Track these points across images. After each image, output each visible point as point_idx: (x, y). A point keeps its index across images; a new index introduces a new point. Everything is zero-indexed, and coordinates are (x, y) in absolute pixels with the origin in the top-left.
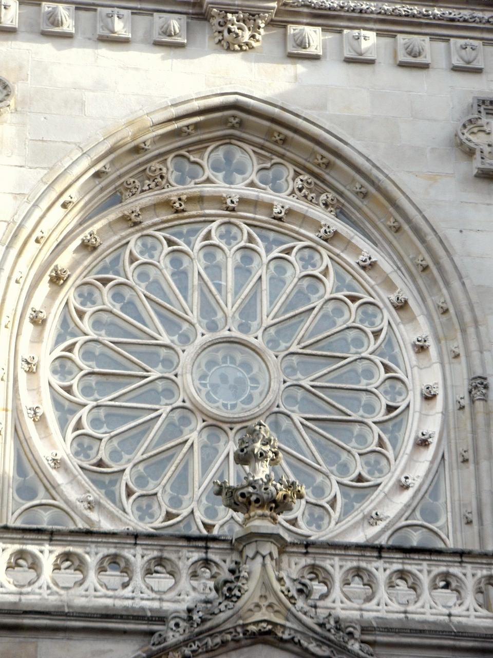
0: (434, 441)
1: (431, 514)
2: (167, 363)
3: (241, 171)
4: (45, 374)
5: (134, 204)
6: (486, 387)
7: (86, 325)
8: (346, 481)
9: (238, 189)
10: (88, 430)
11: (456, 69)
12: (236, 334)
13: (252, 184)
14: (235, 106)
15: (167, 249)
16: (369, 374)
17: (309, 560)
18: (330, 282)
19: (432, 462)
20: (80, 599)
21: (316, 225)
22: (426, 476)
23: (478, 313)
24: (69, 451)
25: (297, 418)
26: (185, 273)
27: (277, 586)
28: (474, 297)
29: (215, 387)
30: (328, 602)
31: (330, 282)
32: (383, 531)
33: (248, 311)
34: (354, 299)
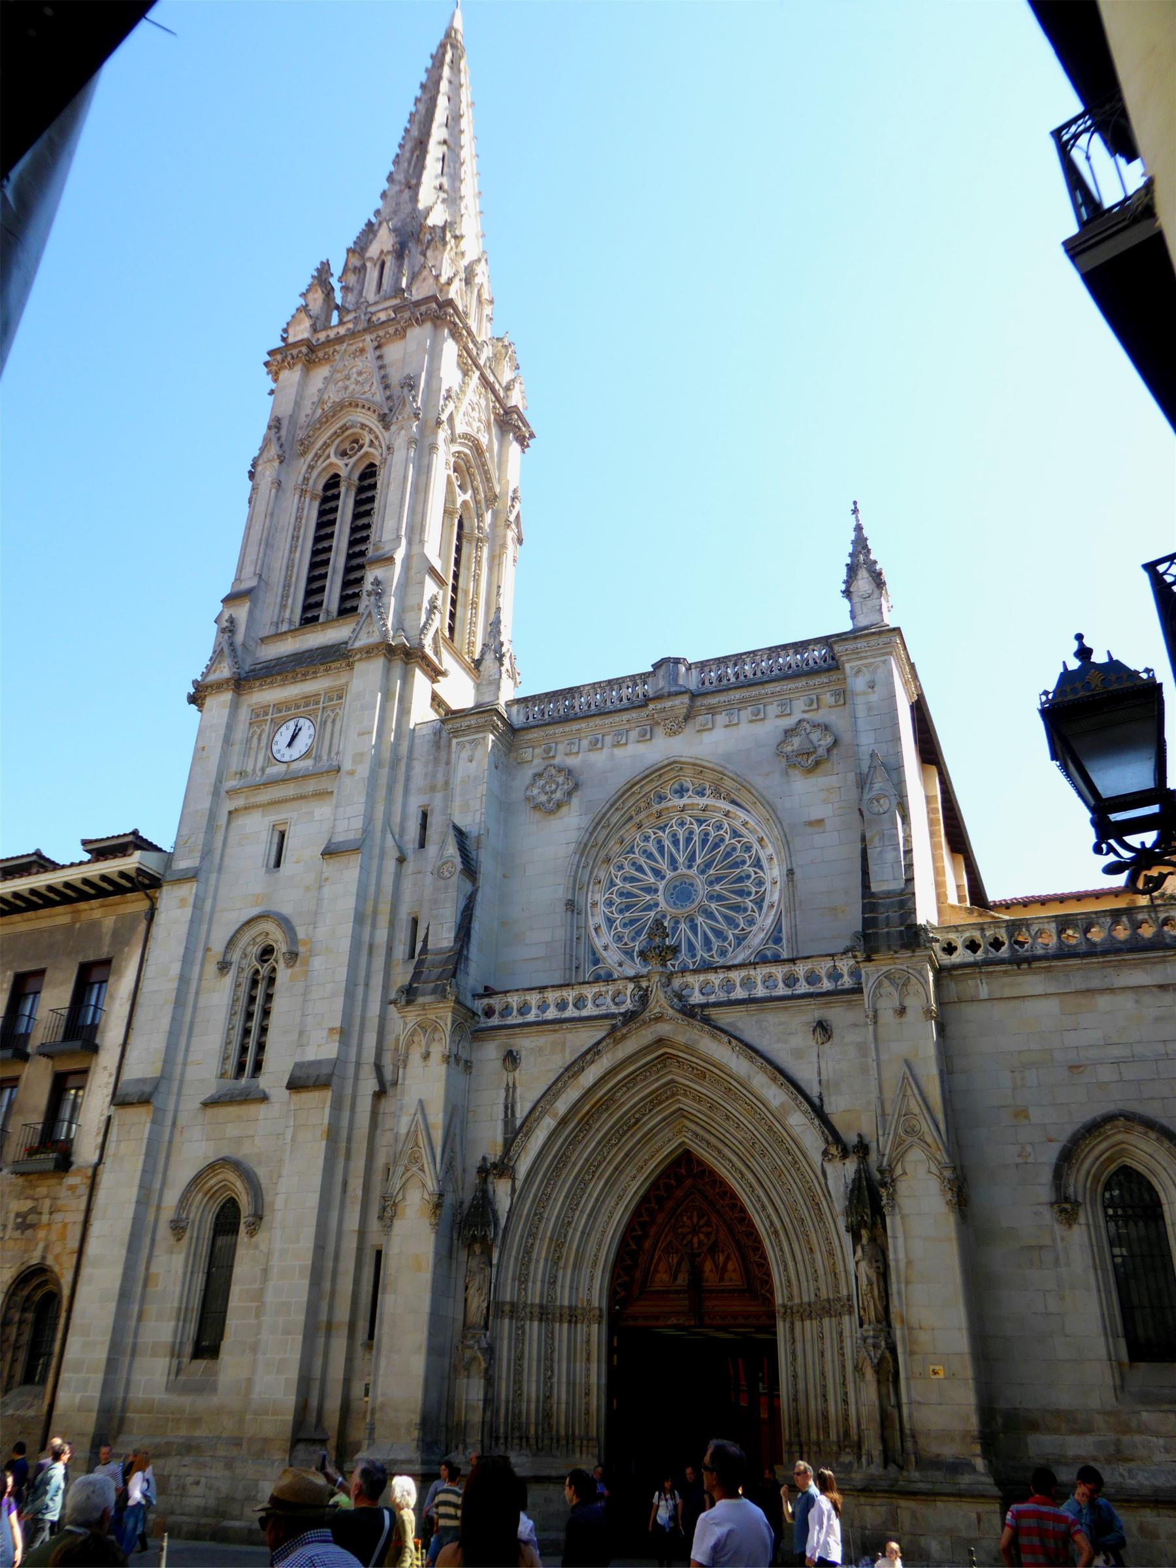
0: (776, 904)
1: (778, 941)
2: (656, 891)
3: (688, 790)
4: (602, 908)
5: (637, 819)
6: (793, 874)
7: (618, 881)
8: (736, 932)
9: (685, 801)
10: (620, 929)
11: (777, 716)
12: (685, 871)
13: (690, 797)
14: (675, 762)
15: (653, 837)
16: (749, 877)
17: (685, 979)
18: (727, 837)
19: (775, 915)
20: (585, 1013)
21: (716, 809)
22: (772, 922)
23: (789, 838)
24: (611, 939)
25: (713, 905)
26: (663, 846)
27: (662, 995)
28: (787, 830)
29: (677, 898)
30: (692, 998)
31: (727, 837)
32: (751, 954)
33: (692, 858)
34: (739, 842)
